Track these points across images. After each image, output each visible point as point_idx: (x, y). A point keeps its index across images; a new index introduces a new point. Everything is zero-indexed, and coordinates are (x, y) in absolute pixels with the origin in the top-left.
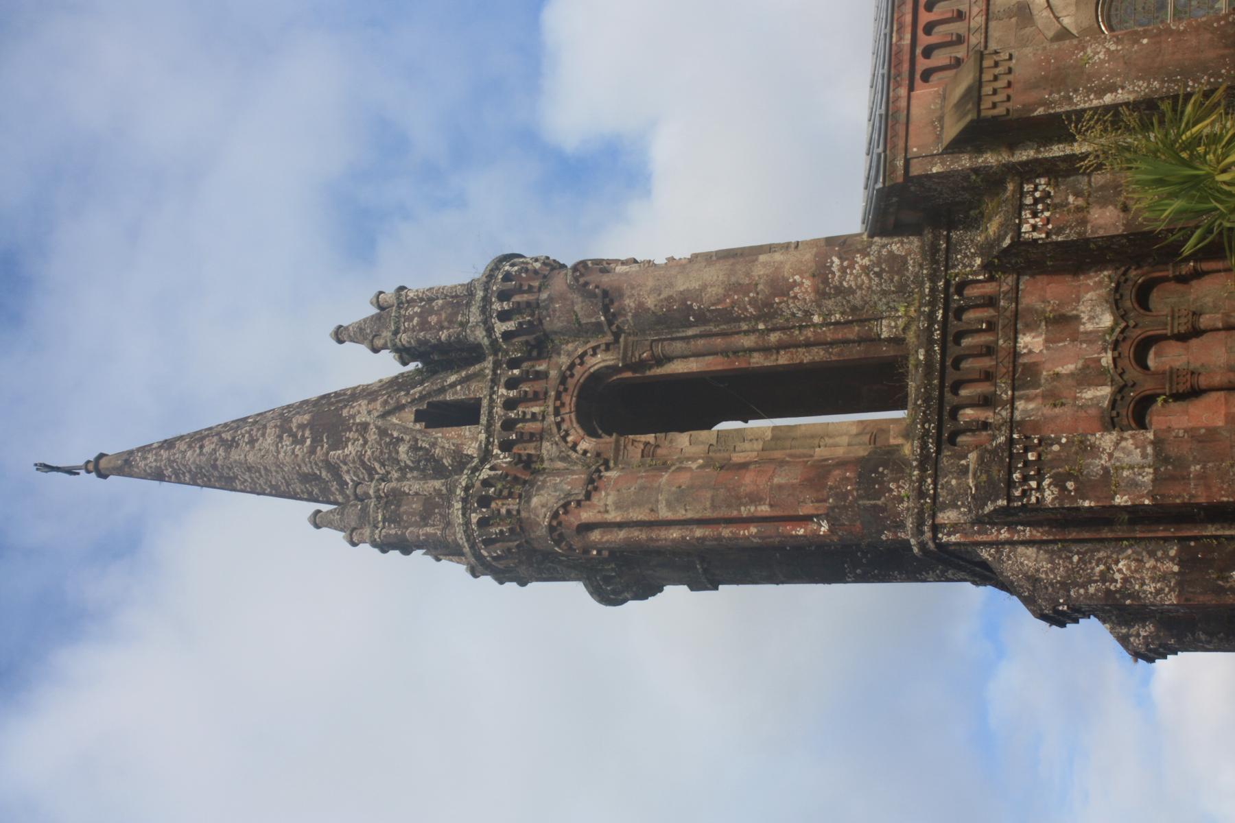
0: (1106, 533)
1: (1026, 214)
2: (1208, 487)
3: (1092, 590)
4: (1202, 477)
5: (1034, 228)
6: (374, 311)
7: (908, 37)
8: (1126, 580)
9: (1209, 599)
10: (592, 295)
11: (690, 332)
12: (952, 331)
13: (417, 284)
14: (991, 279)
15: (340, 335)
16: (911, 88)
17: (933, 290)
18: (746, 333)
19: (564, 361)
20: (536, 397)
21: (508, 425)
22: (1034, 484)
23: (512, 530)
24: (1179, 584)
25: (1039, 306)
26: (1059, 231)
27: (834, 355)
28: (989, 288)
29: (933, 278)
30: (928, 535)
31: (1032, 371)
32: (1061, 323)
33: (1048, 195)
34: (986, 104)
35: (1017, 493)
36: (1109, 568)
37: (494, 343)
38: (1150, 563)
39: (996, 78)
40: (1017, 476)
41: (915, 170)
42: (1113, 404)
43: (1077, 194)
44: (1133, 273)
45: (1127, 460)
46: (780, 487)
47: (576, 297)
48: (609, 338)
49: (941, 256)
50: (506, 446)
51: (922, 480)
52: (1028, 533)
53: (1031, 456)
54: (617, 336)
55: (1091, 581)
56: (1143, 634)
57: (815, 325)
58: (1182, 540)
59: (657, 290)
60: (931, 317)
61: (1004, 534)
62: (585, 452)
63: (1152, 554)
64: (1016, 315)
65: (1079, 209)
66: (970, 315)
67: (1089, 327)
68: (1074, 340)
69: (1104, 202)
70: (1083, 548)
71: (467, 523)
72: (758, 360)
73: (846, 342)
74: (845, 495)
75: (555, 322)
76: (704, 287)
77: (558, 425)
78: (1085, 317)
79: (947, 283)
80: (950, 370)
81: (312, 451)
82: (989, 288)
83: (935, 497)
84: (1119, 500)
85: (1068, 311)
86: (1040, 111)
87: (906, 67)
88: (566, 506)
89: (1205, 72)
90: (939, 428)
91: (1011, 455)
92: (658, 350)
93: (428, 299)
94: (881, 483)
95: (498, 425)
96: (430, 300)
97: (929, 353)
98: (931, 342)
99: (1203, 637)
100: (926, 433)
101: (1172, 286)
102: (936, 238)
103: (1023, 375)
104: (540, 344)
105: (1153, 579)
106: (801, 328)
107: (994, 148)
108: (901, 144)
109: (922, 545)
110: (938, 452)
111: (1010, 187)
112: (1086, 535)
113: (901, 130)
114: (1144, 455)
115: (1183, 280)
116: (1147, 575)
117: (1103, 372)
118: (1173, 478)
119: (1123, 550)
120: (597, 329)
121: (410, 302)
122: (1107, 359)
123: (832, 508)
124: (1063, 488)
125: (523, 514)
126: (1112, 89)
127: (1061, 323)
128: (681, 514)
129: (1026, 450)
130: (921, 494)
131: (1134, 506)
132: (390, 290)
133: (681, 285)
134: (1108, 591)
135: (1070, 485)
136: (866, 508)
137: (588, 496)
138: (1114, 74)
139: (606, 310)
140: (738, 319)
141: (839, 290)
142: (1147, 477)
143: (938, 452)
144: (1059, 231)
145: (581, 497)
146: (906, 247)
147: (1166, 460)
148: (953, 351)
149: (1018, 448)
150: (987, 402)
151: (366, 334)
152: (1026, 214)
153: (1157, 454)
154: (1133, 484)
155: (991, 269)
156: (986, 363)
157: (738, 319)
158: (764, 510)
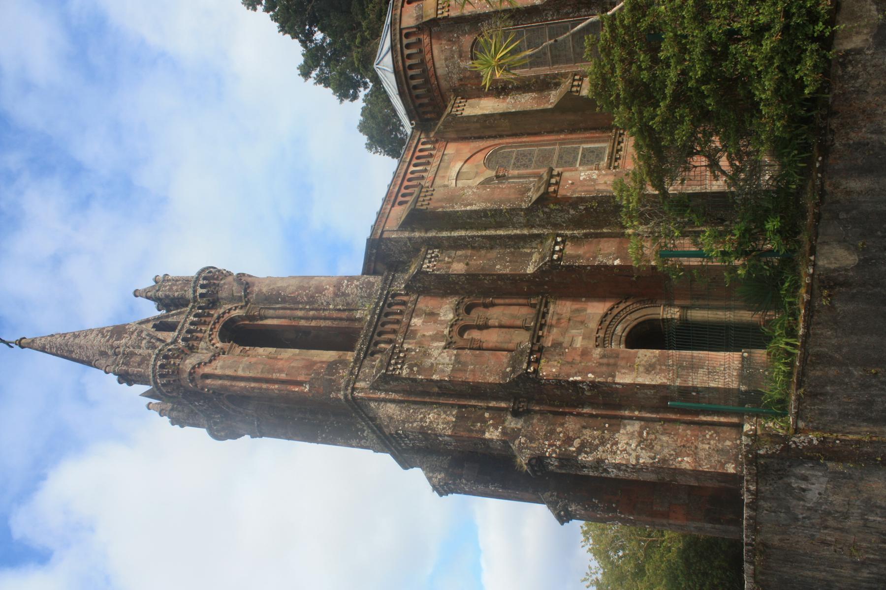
0: (427, 399)
1: (427, 261)
2: (474, 375)
3: (415, 425)
4: (473, 371)
5: (428, 267)
6: (154, 283)
7: (397, 188)
8: (431, 422)
9: (465, 434)
10: (242, 284)
11: (278, 306)
12: (385, 311)
13: (173, 273)
14: (407, 294)
15: (136, 294)
16: (393, 206)
17: (381, 294)
18: (301, 309)
19: (221, 311)
22: (399, 366)
23: (173, 372)
24: (454, 426)
25: (424, 308)
26: (438, 270)
27: (335, 324)
28: (405, 298)
29: (383, 289)
30: (350, 391)
31: (414, 332)
32: (432, 315)
33: (437, 256)
34: (419, 204)
35: (391, 368)
36: (425, 417)
37: (195, 297)
38: (443, 416)
39: (425, 196)
40: (393, 362)
41: (385, 235)
43: (449, 257)
44: (466, 300)
45: (442, 361)
46: (293, 367)
47: (235, 284)
48: (244, 304)
49: (389, 282)
50: (184, 340)
51: (353, 368)
52: (393, 396)
53: (402, 355)
54: (247, 303)
55: (415, 421)
57: (330, 310)
58: (460, 407)
59: (269, 285)
60: (377, 304)
61: (383, 395)
63: (445, 412)
64: (414, 310)
65: (449, 263)
66: (395, 308)
67: (443, 318)
68: (435, 322)
69: (459, 261)
70: (416, 407)
71: (155, 365)
72: (303, 323)
73: (341, 319)
74: (319, 374)
75: (223, 294)
76: (288, 286)
77: (210, 335)
78: (442, 314)
79: (388, 293)
80: (379, 326)
81: (108, 341)
82: (405, 298)
83: (357, 376)
84: (435, 377)
85: (435, 311)
86: (440, 210)
87: (393, 198)
89: (509, 202)
90: (368, 348)
91: (393, 353)
92: (262, 312)
93: (176, 280)
94: (336, 370)
96: (177, 281)
97: (372, 317)
98: (374, 313)
99: (464, 481)
100: (361, 349)
101: (481, 309)
102: (389, 275)
103: (409, 333)
104: (214, 303)
105: (443, 423)
106: (324, 310)
107: (420, 230)
108: (382, 225)
109: (346, 396)
110: (364, 358)
111: (423, 250)
112: (418, 399)
113: (384, 220)
114: (450, 360)
115: (486, 306)
116: (440, 421)
117: (444, 336)
118: (460, 370)
119: (433, 409)
120: (240, 299)
121: (168, 281)
122: (446, 332)
123: (312, 379)
124: (412, 370)
125: (181, 366)
126: (471, 204)
127: (432, 315)
128: (248, 374)
129: (400, 352)
130: (351, 373)
131: (441, 380)
132: (161, 275)
133: (279, 284)
134: (422, 426)
135: (415, 369)
136: (327, 380)
137: (210, 361)
138: (473, 200)
139: (245, 290)
140: (299, 303)
141: (344, 294)
142: (449, 369)
143: (364, 358)
144: (438, 270)
145: (207, 361)
146: (376, 281)
147: (459, 363)
148: (384, 319)
149: (397, 350)
151: (147, 294)
152: (427, 261)
153: (456, 360)
154: (443, 371)
155: (409, 288)
156: (396, 327)
157: (299, 303)
158: (283, 376)
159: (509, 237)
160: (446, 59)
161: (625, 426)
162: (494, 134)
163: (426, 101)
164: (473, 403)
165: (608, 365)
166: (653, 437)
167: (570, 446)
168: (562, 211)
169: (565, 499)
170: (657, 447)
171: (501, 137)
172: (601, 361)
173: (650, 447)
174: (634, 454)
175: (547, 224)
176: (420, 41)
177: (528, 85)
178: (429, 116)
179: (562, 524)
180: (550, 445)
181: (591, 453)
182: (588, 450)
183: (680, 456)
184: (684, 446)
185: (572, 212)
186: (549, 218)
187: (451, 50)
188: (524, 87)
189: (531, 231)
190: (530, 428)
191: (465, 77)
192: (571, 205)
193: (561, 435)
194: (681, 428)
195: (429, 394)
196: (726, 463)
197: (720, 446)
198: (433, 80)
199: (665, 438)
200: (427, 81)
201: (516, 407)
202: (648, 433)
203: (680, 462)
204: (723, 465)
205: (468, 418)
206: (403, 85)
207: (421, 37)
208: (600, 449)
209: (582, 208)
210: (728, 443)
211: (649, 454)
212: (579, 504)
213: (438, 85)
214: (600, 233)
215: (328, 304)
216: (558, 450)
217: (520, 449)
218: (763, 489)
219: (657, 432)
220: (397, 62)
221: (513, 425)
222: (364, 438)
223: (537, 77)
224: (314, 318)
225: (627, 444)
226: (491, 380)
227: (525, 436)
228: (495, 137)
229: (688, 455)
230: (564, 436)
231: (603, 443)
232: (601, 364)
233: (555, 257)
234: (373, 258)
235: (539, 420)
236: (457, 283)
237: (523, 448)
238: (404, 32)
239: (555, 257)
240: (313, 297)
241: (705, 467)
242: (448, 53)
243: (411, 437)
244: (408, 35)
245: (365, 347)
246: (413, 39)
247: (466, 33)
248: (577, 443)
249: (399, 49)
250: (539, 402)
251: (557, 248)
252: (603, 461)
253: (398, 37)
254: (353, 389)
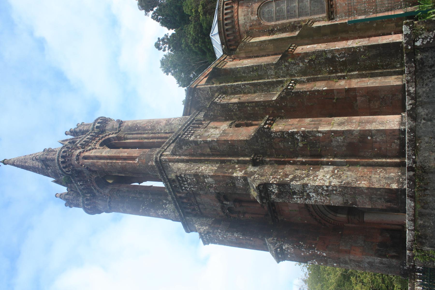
3: (192, 171)
23: (69, 155)
30: (159, 155)
40: (186, 134)
44: (236, 122)
54: (119, 131)
55: (193, 170)
56: (204, 228)
57: (161, 133)
60: (186, 122)
63: (212, 166)
79: (194, 119)
99: (219, 231)
100: (172, 139)
102: (196, 112)
104: (103, 131)
106: (159, 133)
109: (156, 158)
134: (196, 172)
136: (149, 154)
140: (146, 130)
157: (146, 130)
159: (265, 84)
160: (244, 16)
161: (323, 168)
162: (265, 54)
163: (232, 38)
164: (230, 158)
165: (314, 124)
166: (342, 172)
167: (286, 178)
168: (295, 64)
169: (282, 241)
170: (344, 177)
171: (268, 55)
172: (310, 123)
173: (340, 177)
174: (328, 181)
175: (287, 75)
176: (232, 7)
177: (285, 28)
178: (232, 48)
179: (278, 262)
180: (273, 178)
181: (299, 181)
182: (298, 179)
183: (359, 181)
184: (362, 176)
185: (301, 65)
186: (288, 70)
187: (248, 11)
188: (283, 29)
189: (277, 79)
190: (262, 171)
191: (253, 25)
192: (300, 59)
193: (281, 173)
194: (360, 169)
195: (204, 155)
196: (391, 183)
197: (387, 176)
198: (237, 27)
199: (349, 173)
200: (233, 27)
201: (255, 158)
202: (338, 171)
203: (359, 184)
204: (389, 185)
205: (224, 168)
206: (221, 28)
207: (234, 5)
208: (306, 179)
209: (306, 61)
210: (392, 174)
211: (338, 180)
212: (290, 244)
213: (239, 29)
214: (317, 77)
215: (161, 130)
216: (278, 180)
217: (254, 180)
218: (420, 91)
219: (345, 170)
220: (220, 16)
221: (252, 170)
222: (166, 209)
223: (290, 23)
224: (152, 138)
225: (324, 176)
226: (242, 138)
227: (259, 174)
228: (265, 56)
229: (365, 181)
230: (283, 174)
231: (308, 176)
232: (310, 124)
233: (289, 87)
234: (189, 104)
235: (268, 167)
236: (233, 111)
237: (255, 180)
238: (225, 3)
239: (289, 87)
240: (154, 126)
241: (377, 186)
242: (246, 13)
243: (189, 181)
244: (227, 5)
245: (174, 139)
246: (229, 6)
247: (256, 2)
248: (291, 177)
249: (221, 10)
250: (269, 156)
251: (291, 84)
252: (307, 185)
253: (222, 4)
254: (161, 155)
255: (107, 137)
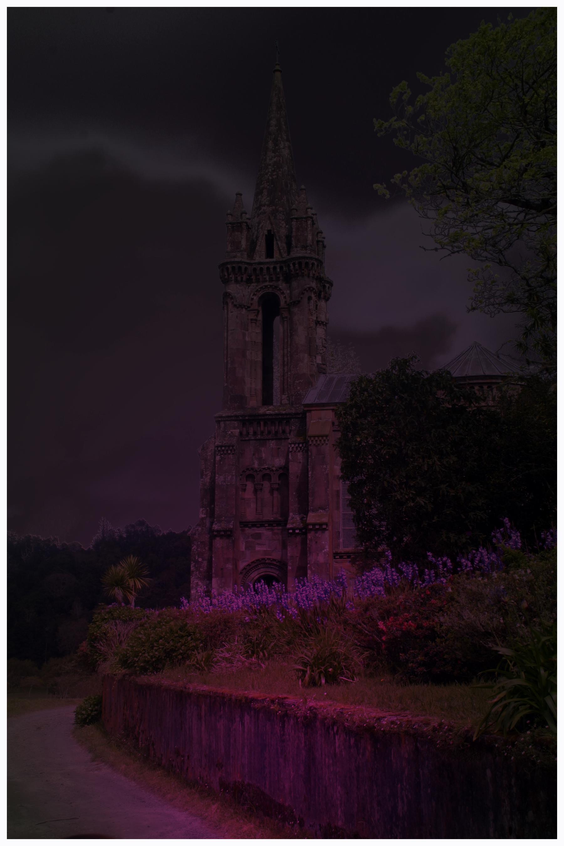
20: (271, 280)
21: (261, 269)
42: (252, 469)
53: (229, 452)
62: (252, 299)
88: (232, 298)
95: (262, 266)
137: (235, 306)
150: (255, 433)
158: (229, 366)
255: (278, 293)
